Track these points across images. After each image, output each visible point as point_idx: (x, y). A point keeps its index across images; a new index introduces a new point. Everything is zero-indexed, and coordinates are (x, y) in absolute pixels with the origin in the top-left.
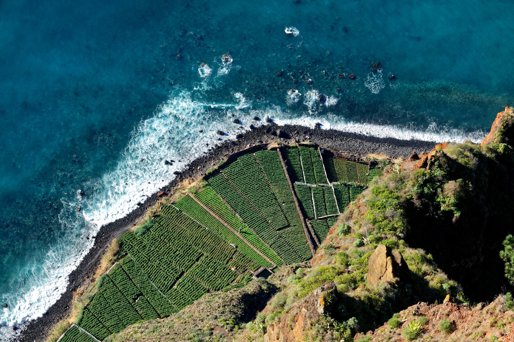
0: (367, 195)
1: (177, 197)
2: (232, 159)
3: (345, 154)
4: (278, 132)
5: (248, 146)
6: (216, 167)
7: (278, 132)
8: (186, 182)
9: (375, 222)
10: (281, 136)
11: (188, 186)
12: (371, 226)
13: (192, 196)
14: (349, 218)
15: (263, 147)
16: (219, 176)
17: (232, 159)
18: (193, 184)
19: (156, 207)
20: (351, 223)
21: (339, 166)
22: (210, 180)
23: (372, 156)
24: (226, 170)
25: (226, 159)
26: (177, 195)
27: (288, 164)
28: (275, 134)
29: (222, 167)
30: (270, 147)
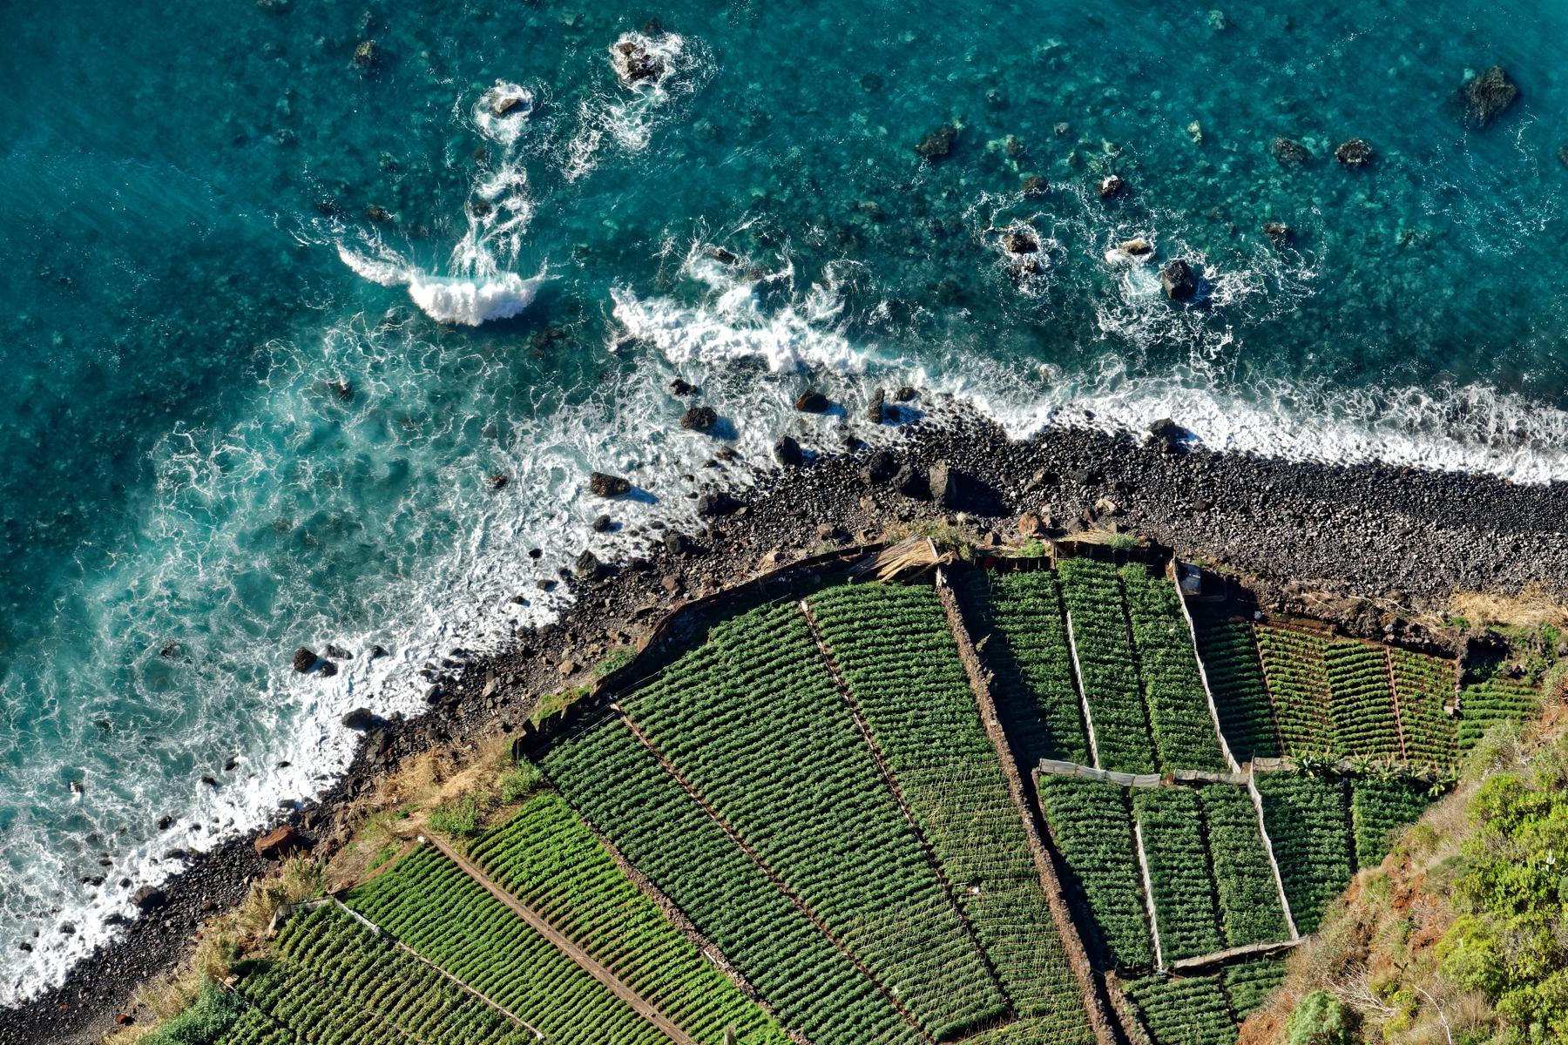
0: (1454, 829)
1: (367, 855)
2: (680, 634)
3: (1321, 597)
4: (938, 475)
5: (769, 562)
6: (587, 683)
7: (938, 475)
8: (415, 772)
9: (1496, 983)
10: (952, 502)
11: (432, 790)
12: (1474, 1006)
13: (453, 850)
14: (1347, 967)
15: (850, 566)
16: (602, 736)
17: (680, 634)
18: (461, 781)
19: (245, 919)
20: (1362, 992)
21: (1292, 664)
22: (556, 758)
23: (1476, 609)
24: (647, 699)
25: (642, 637)
26: (367, 844)
27: (998, 657)
28: (918, 488)
29: (622, 682)
30: (892, 563)
